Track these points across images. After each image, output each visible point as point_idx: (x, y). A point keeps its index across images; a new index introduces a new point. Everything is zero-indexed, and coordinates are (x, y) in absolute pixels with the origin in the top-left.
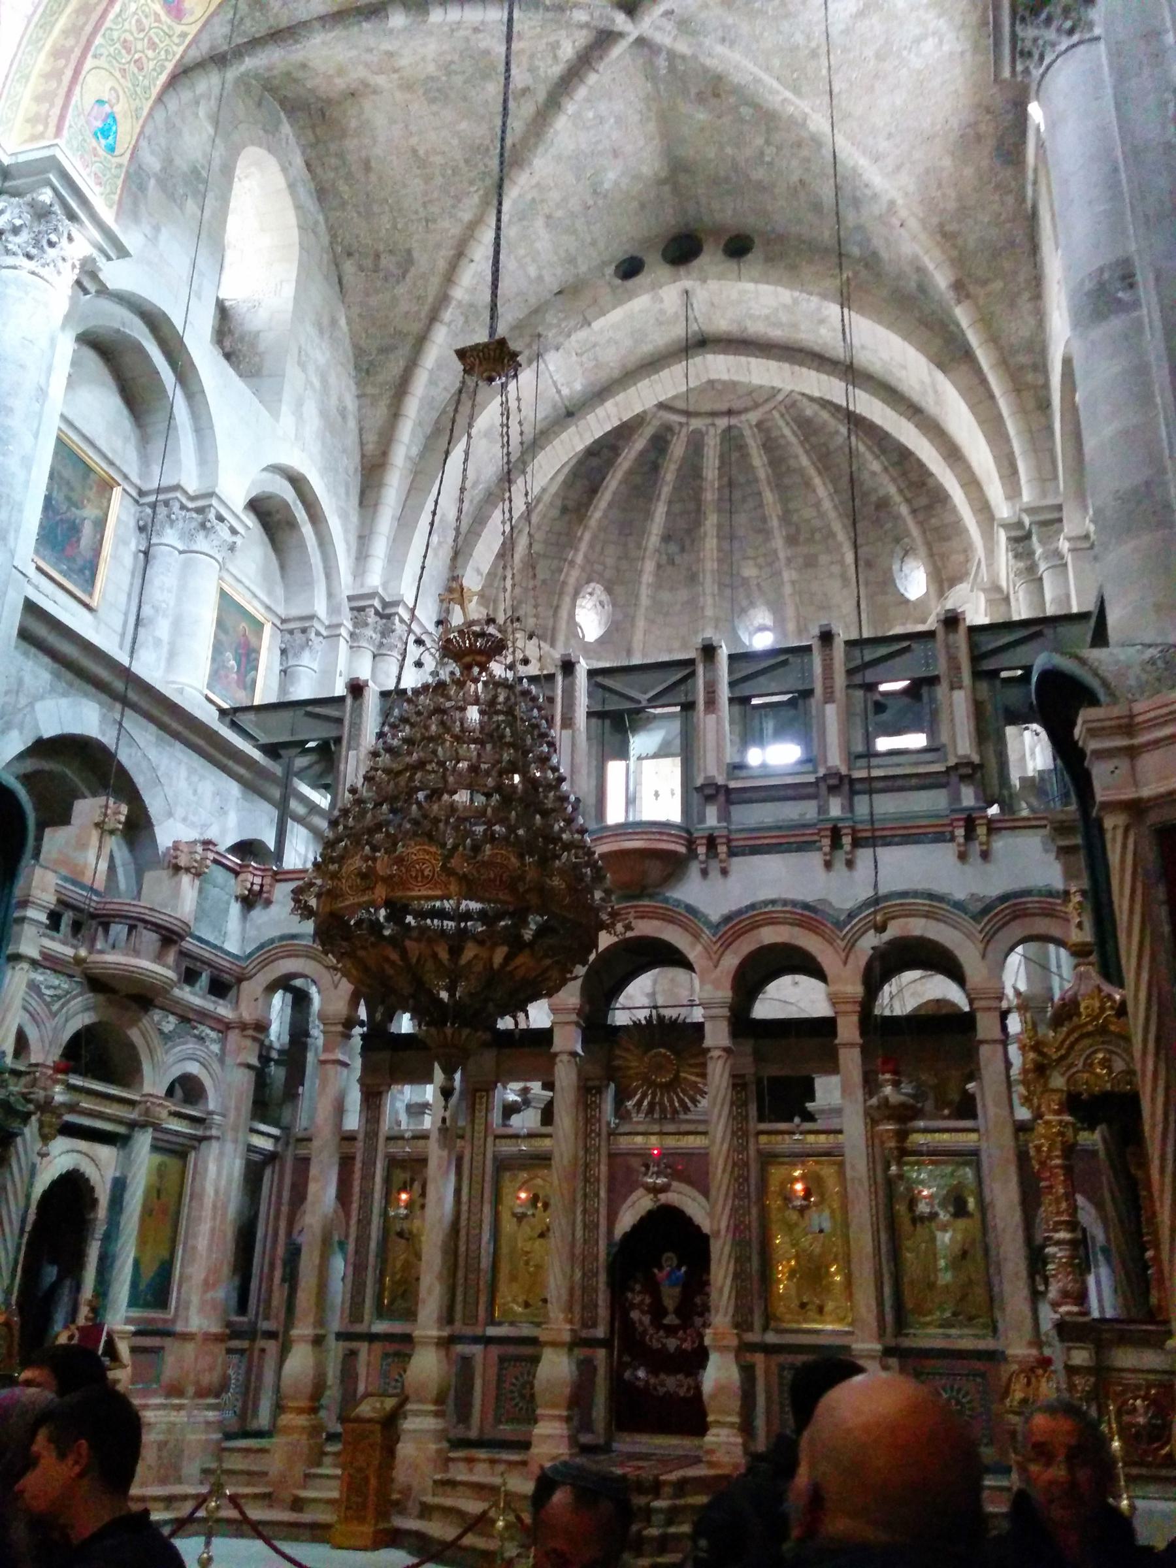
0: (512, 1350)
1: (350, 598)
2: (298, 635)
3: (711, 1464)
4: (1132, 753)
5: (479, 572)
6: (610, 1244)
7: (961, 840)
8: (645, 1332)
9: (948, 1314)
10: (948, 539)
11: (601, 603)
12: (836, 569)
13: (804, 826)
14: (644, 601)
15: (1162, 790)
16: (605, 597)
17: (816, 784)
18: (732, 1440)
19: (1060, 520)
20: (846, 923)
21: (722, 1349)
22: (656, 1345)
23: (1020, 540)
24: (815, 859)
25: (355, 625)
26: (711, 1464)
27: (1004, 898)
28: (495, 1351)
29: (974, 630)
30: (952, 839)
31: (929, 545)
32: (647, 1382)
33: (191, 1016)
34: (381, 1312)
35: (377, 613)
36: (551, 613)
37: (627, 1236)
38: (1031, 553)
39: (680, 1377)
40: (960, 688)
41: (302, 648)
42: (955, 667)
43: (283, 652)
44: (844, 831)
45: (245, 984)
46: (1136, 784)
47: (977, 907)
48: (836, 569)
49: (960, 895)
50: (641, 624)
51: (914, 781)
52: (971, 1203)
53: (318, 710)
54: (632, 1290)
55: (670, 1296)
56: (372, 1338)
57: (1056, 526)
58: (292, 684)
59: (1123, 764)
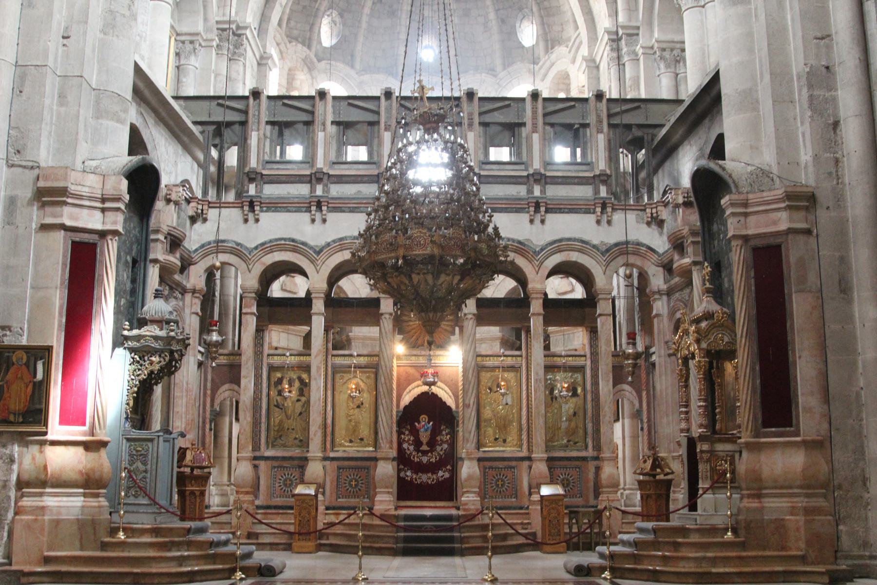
0: (346, 463)
1: (217, 22)
2: (189, 47)
3: (465, 510)
4: (746, 215)
5: (281, 4)
6: (397, 412)
7: (599, 214)
8: (411, 453)
9: (565, 441)
10: (554, 15)
11: (334, 21)
12: (481, 20)
13: (520, 199)
14: (364, 25)
15: (756, 232)
16: (338, 19)
17: (528, 176)
18: (475, 498)
19: (638, 35)
20: (539, 253)
21: (470, 459)
22: (416, 460)
23: (615, 40)
24: (525, 217)
25: (220, 40)
26: (465, 510)
27: (617, 245)
28: (335, 464)
29: (610, 100)
30: (594, 213)
31: (541, 17)
32: (412, 478)
33: (174, 286)
34: (272, 443)
35: (234, 33)
36: (308, 28)
37: (406, 407)
38: (618, 50)
39: (430, 475)
40: (602, 132)
41: (190, 53)
42: (600, 121)
43: (177, 54)
44: (541, 204)
45: (192, 267)
46: (746, 228)
47: (604, 248)
48: (481, 20)
49: (595, 242)
50: (361, 39)
51: (576, 181)
52: (579, 390)
53: (228, 103)
54: (404, 434)
55: (424, 437)
56: (267, 458)
57: (635, 37)
58: (185, 77)
59: (742, 219)
